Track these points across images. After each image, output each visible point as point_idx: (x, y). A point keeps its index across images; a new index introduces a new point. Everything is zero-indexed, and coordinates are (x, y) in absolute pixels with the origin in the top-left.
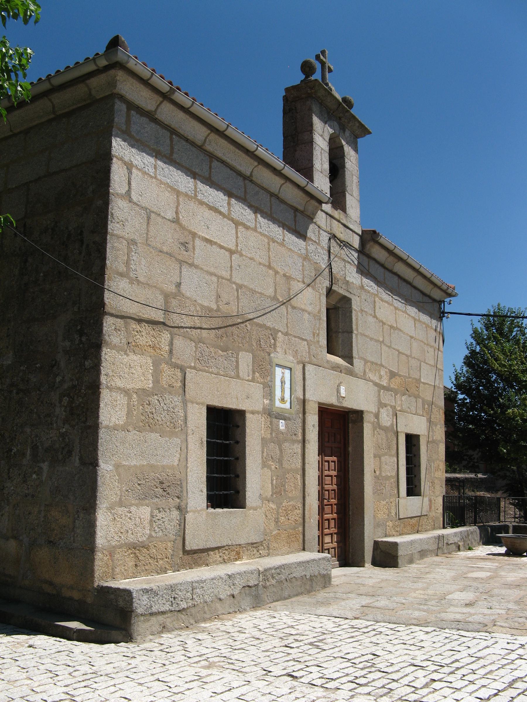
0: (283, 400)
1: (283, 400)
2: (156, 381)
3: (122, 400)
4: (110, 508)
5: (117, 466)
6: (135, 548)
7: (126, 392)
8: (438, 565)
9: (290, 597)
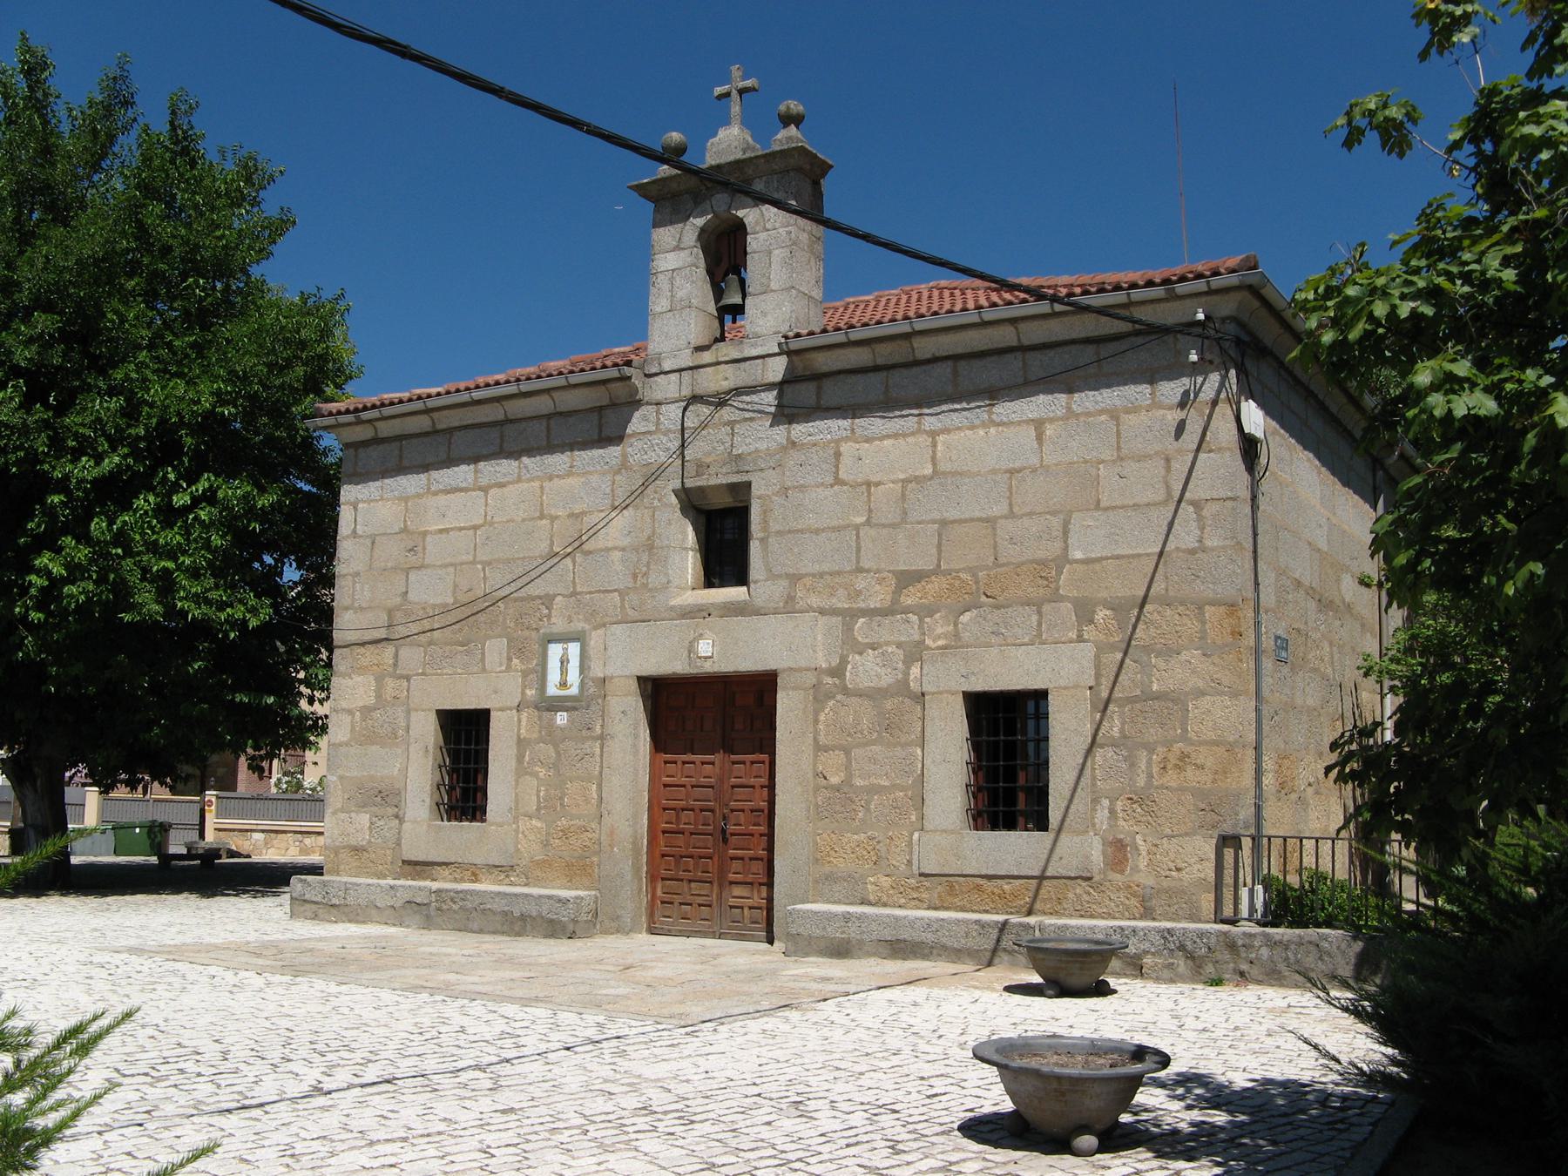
0: (563, 684)
1: (563, 684)
2: (379, 696)
3: (347, 719)
4: (334, 813)
5: (341, 778)
6: (357, 850)
7: (350, 712)
8: (146, 904)
9: (481, 931)
